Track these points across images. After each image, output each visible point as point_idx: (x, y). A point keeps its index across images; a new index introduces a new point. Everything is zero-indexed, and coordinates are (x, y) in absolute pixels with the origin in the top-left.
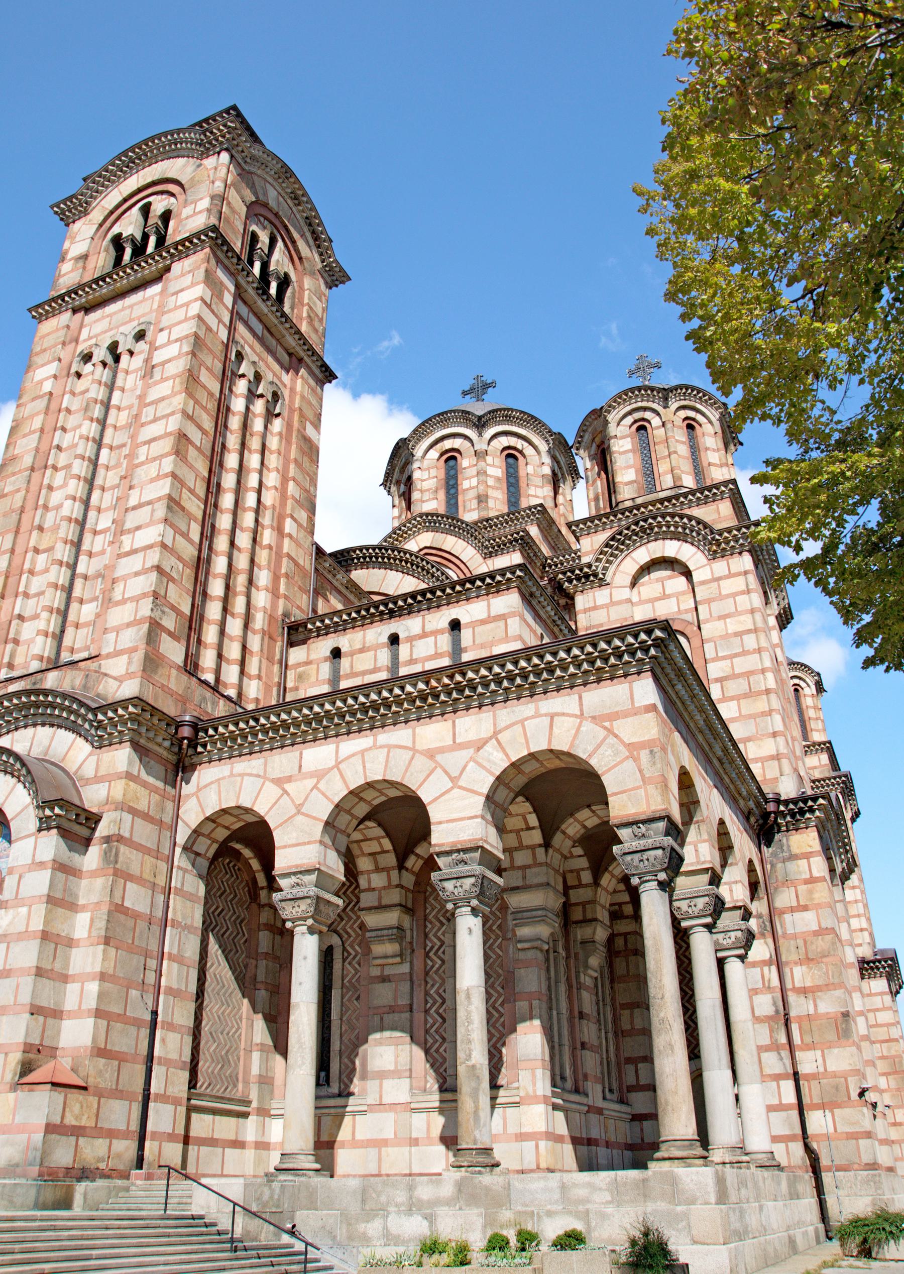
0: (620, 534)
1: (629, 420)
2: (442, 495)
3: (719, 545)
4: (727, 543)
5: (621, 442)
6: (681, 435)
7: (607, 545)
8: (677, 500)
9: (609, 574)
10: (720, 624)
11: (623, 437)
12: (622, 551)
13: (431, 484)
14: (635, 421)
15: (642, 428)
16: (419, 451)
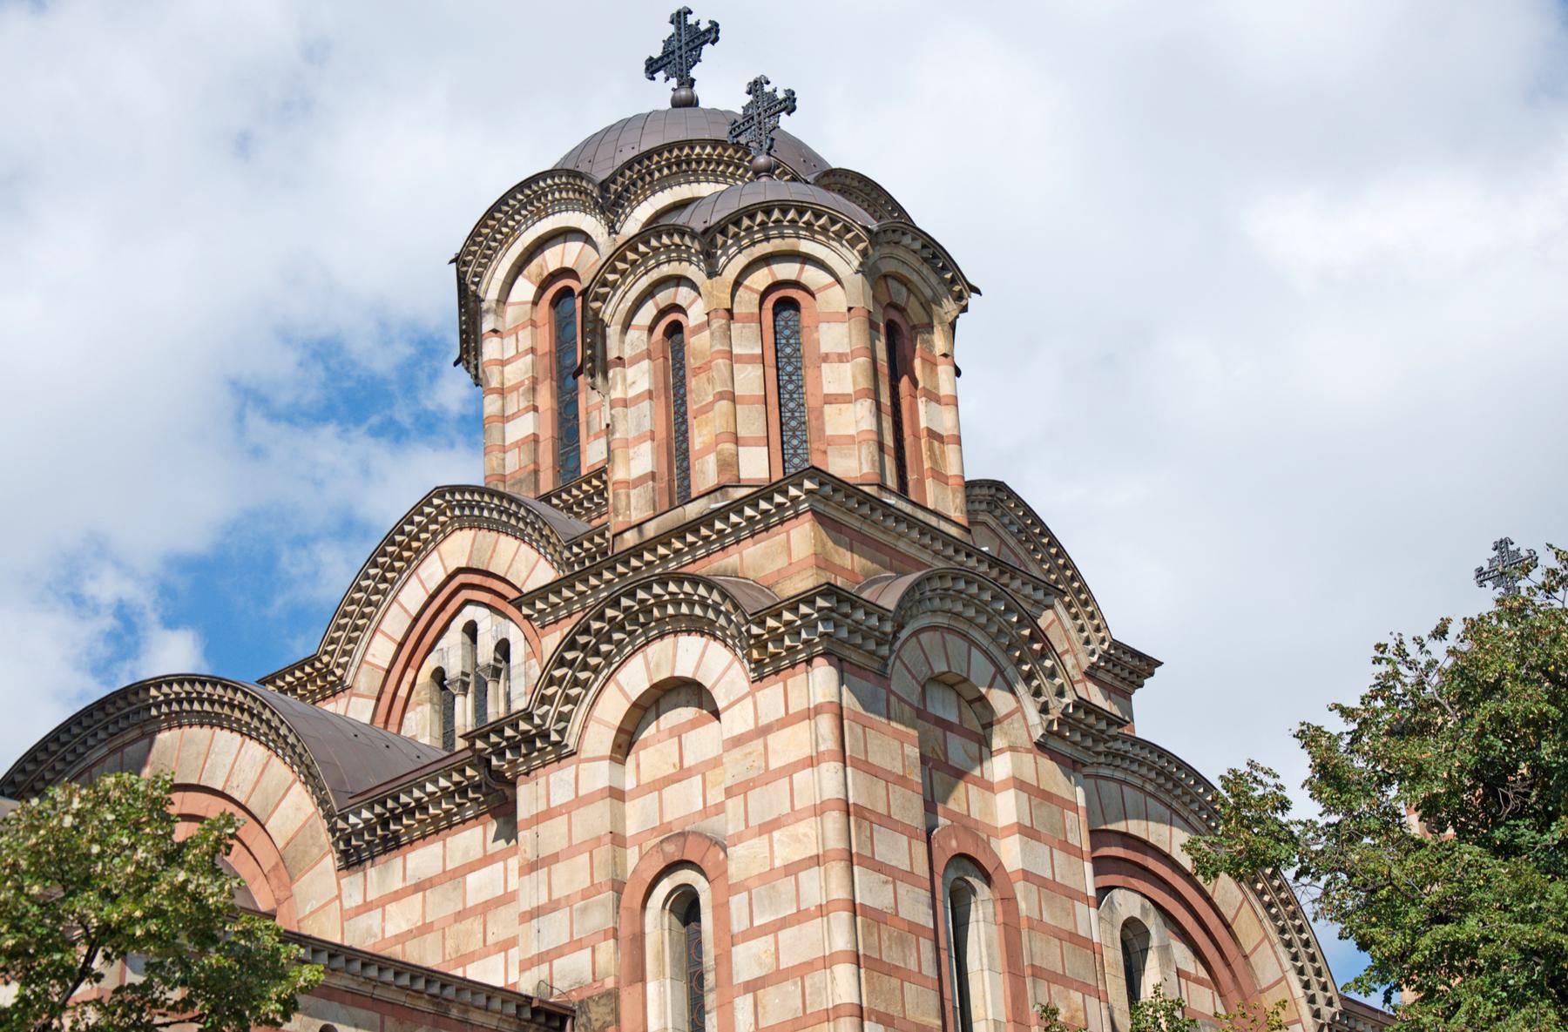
0: (586, 630)
2: (545, 398)
3: (763, 646)
4: (779, 640)
5: (631, 372)
6: (747, 341)
7: (561, 662)
8: (711, 526)
9: (574, 728)
10: (758, 845)
11: (636, 360)
12: (596, 670)
13: (518, 372)
14: (662, 313)
15: (675, 329)
16: (491, 293)
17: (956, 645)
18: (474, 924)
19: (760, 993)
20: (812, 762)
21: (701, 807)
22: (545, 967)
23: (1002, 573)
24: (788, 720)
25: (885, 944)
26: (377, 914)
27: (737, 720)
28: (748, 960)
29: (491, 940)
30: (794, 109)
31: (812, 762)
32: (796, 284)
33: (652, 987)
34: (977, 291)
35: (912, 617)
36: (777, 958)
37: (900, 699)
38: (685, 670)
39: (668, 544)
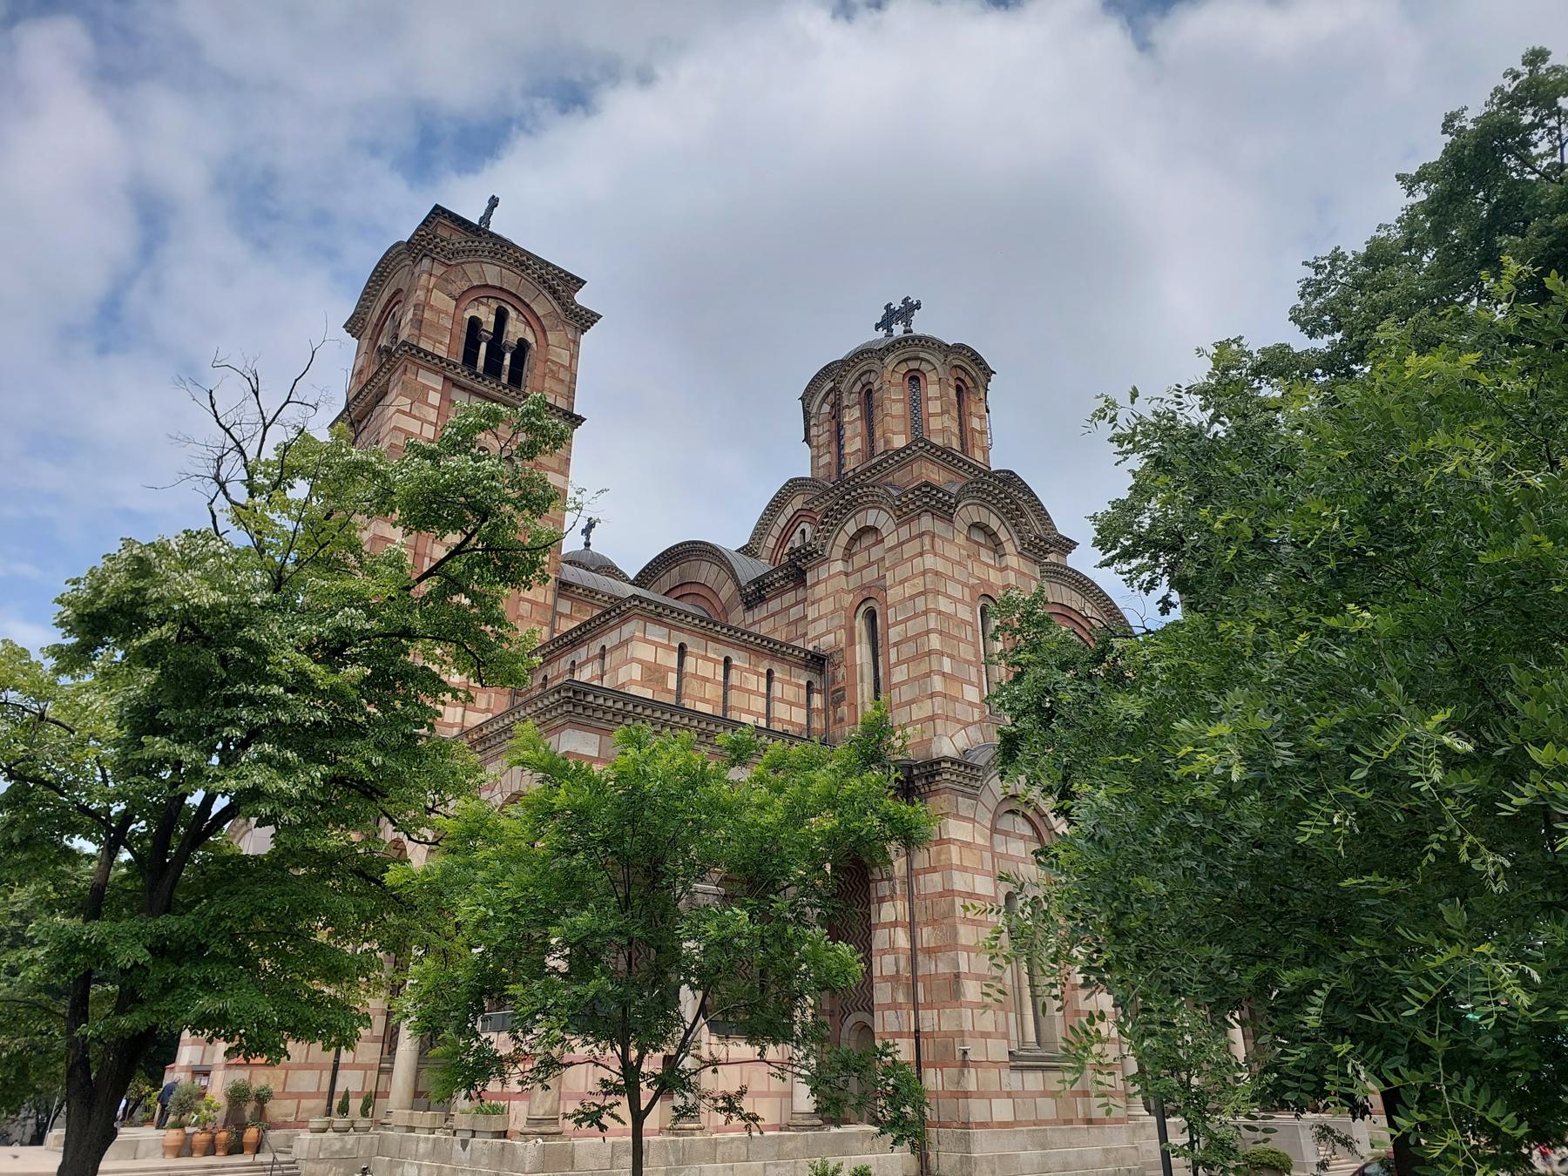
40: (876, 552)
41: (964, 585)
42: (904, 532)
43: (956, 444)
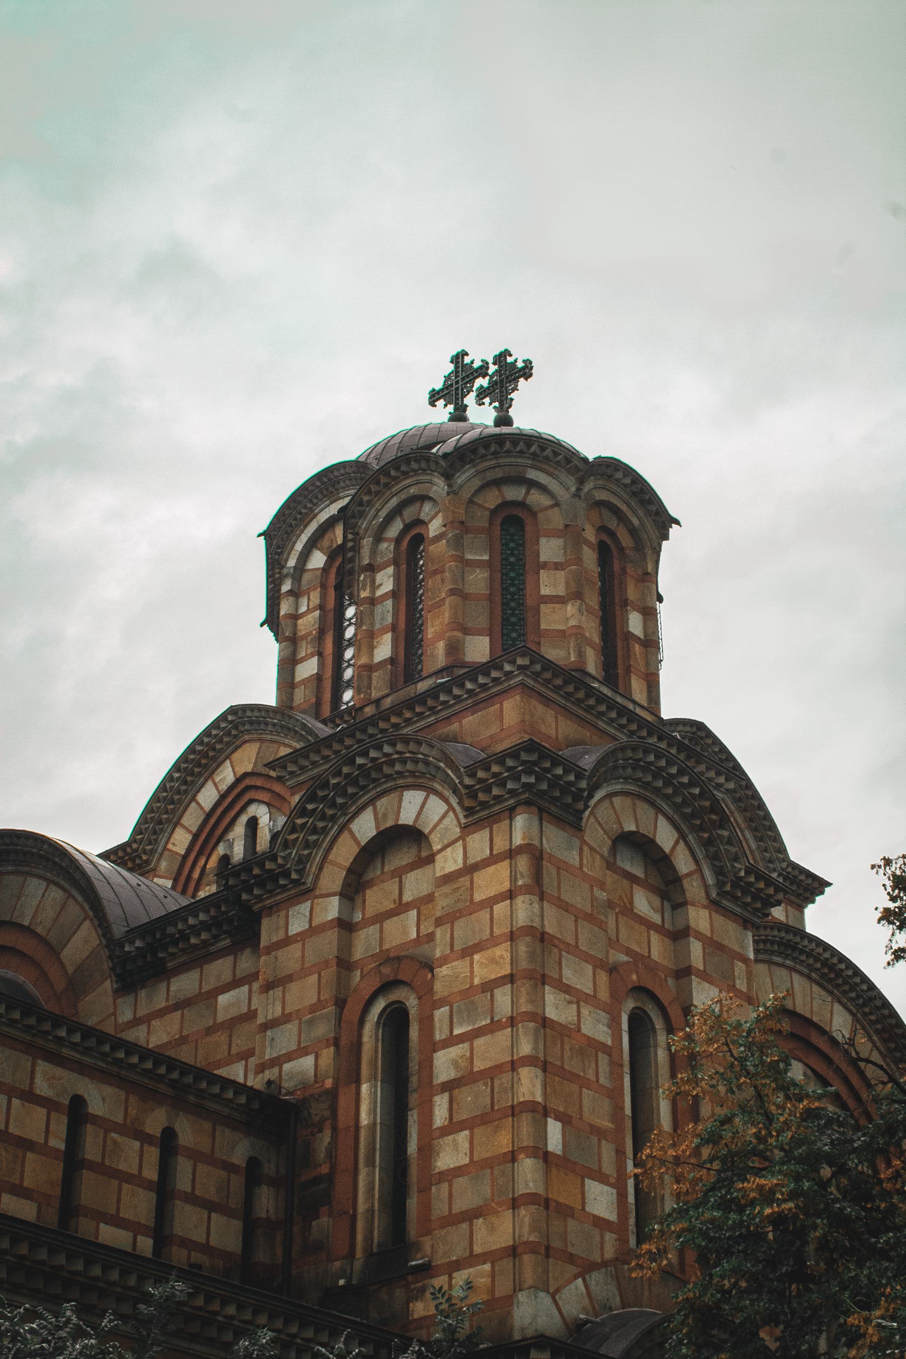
1: (396, 527)
3: (473, 795)
10: (460, 966)
14: (407, 527)
15: (419, 539)
17: (644, 809)
18: (221, 1037)
19: (456, 1092)
20: (511, 895)
21: (414, 935)
22: (276, 1070)
23: (688, 757)
24: (492, 860)
25: (567, 1054)
26: (143, 1028)
27: (450, 861)
28: (445, 1065)
29: (234, 1051)
30: (531, 375)
31: (511, 895)
32: (522, 505)
33: (365, 1088)
34: (677, 522)
35: (606, 781)
36: (472, 1062)
37: (592, 849)
38: (407, 817)
39: (400, 714)
40: (416, 884)
41: (599, 964)
42: (479, 844)
43: (592, 664)
